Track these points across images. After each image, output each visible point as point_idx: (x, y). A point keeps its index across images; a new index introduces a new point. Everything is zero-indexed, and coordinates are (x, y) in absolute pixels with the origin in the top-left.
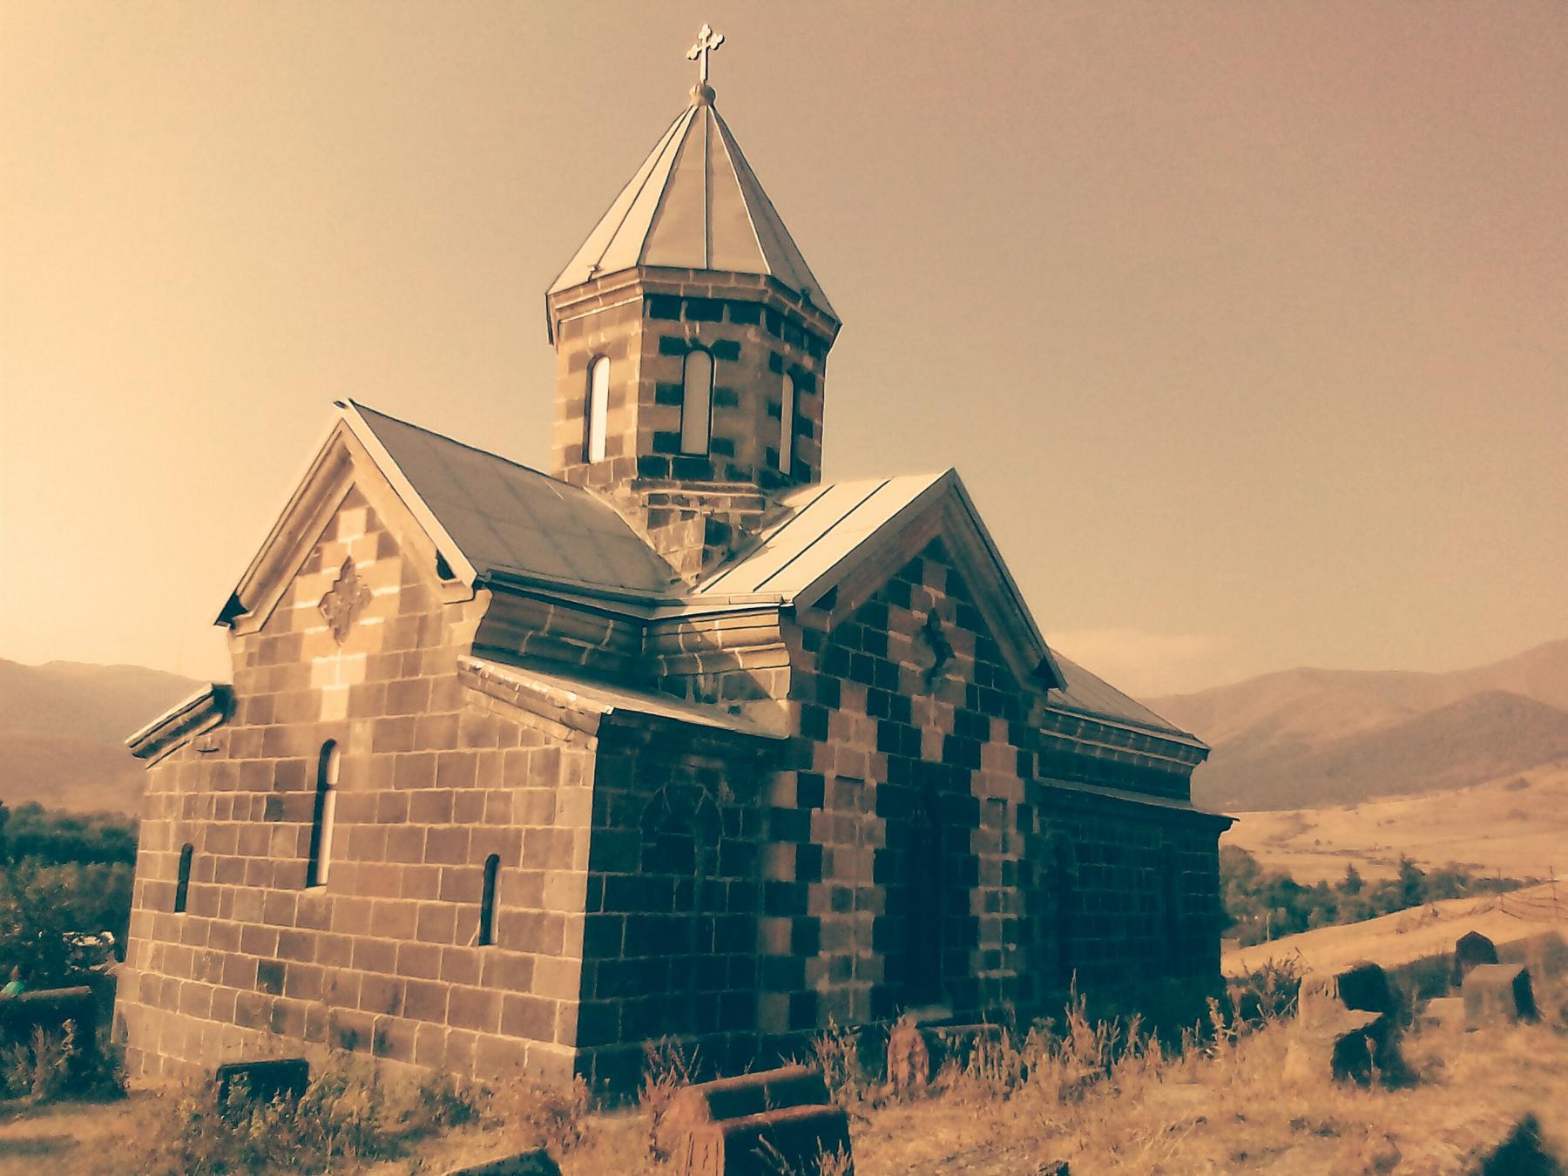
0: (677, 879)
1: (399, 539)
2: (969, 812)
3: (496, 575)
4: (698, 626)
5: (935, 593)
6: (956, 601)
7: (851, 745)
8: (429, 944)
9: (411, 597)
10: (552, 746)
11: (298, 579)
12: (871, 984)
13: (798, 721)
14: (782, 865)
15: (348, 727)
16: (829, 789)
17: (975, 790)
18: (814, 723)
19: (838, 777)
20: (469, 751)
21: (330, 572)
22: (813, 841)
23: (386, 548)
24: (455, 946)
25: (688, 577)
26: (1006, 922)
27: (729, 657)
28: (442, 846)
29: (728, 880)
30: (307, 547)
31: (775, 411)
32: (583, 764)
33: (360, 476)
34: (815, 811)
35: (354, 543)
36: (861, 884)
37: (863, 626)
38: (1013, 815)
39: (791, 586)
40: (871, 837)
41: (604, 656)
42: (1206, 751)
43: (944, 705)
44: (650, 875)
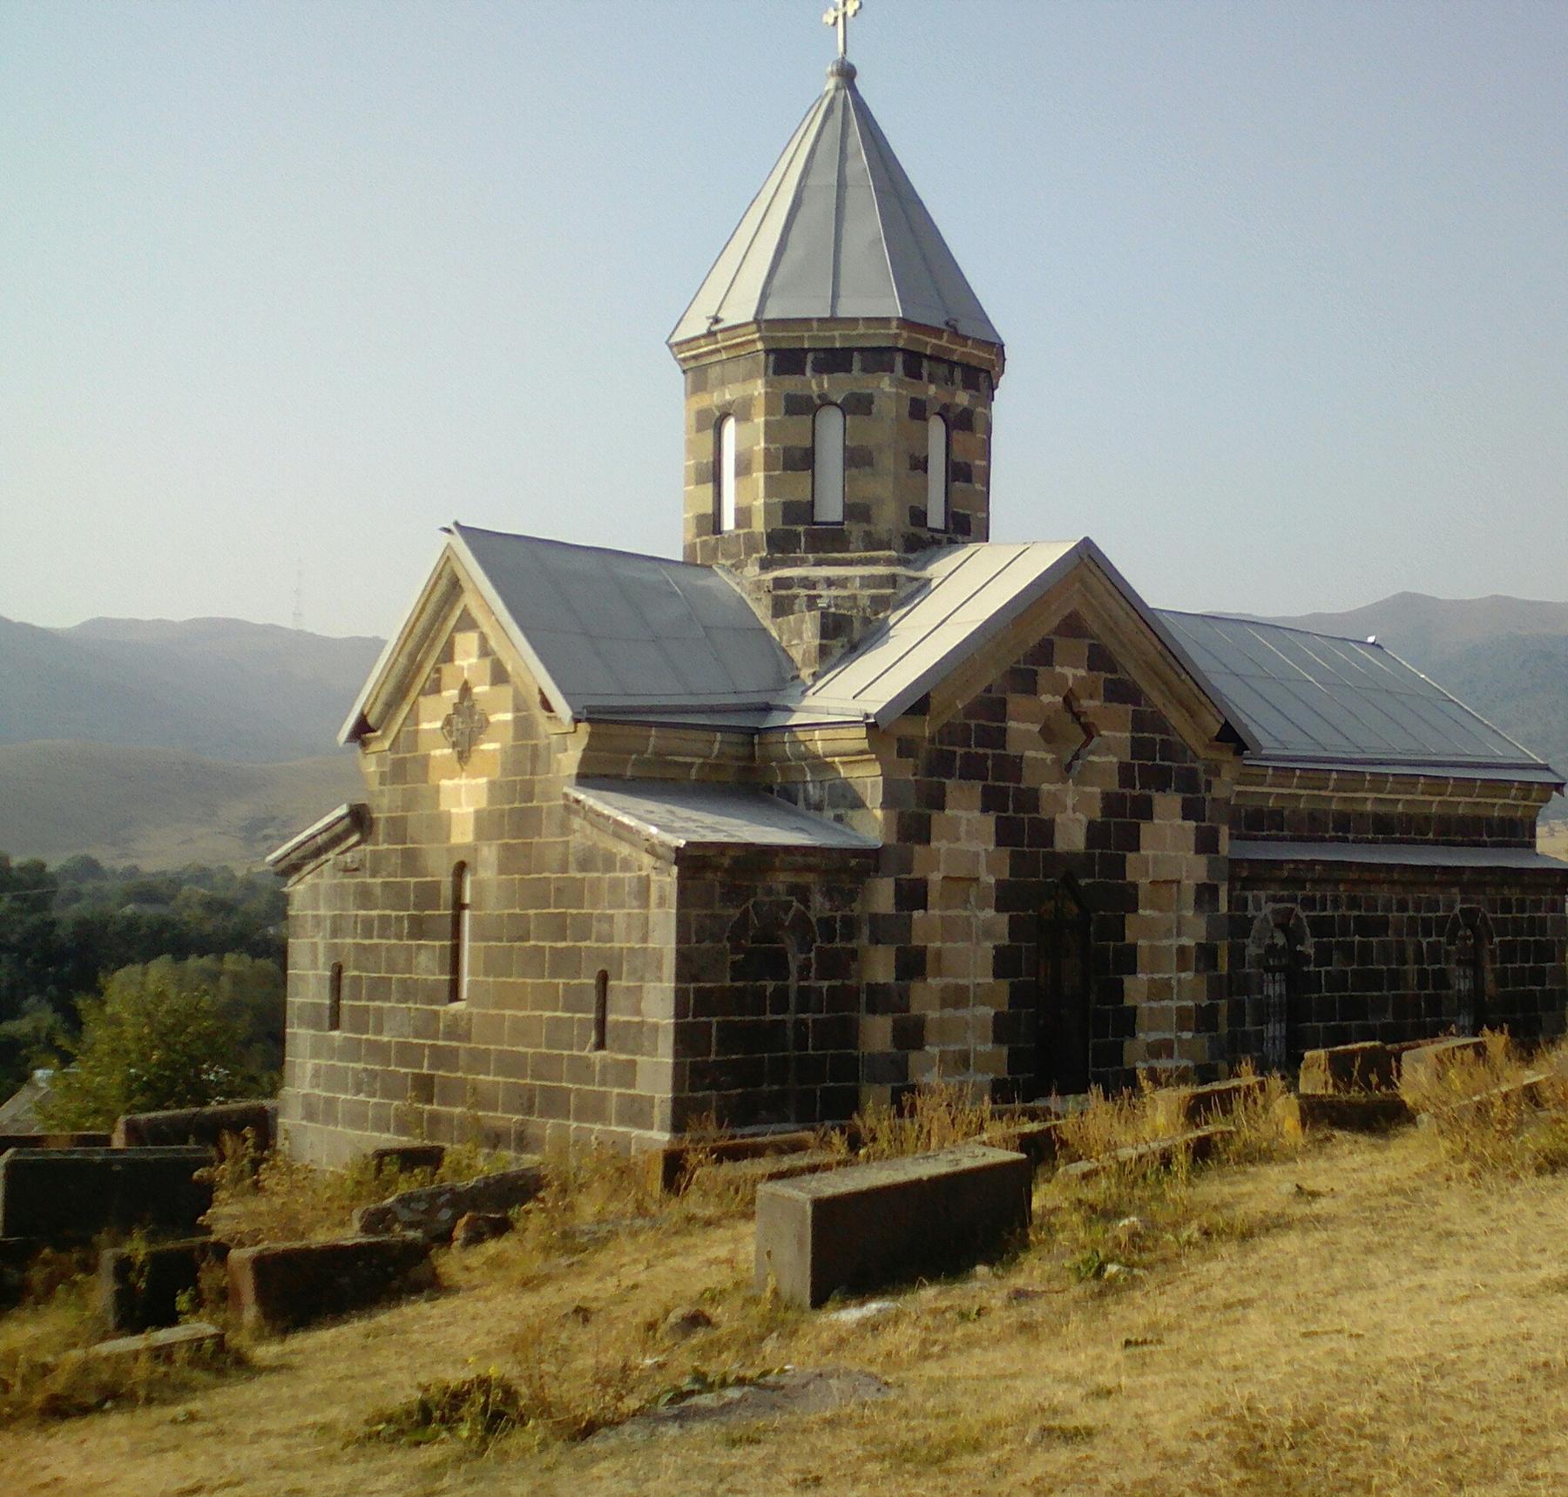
0: (770, 985)
1: (509, 668)
2: (1128, 899)
3: (591, 710)
4: (801, 736)
5: (1072, 673)
6: (1104, 675)
7: (963, 845)
8: (556, 1052)
9: (524, 726)
10: (644, 873)
11: (421, 699)
12: (992, 1076)
13: (895, 828)
14: (880, 967)
15: (476, 850)
16: (933, 895)
18: (914, 828)
20: (579, 875)
21: (451, 694)
22: (915, 943)
23: (499, 676)
24: (575, 1053)
25: (805, 673)
27: (831, 766)
28: (564, 962)
29: (826, 984)
30: (427, 668)
32: (668, 889)
33: (468, 600)
34: (918, 914)
35: (470, 666)
36: (980, 980)
37: (973, 723)
38: (1190, 897)
39: (876, 701)
40: (988, 934)
41: (717, 767)
42: (1559, 787)
43: (1088, 789)
44: (739, 984)
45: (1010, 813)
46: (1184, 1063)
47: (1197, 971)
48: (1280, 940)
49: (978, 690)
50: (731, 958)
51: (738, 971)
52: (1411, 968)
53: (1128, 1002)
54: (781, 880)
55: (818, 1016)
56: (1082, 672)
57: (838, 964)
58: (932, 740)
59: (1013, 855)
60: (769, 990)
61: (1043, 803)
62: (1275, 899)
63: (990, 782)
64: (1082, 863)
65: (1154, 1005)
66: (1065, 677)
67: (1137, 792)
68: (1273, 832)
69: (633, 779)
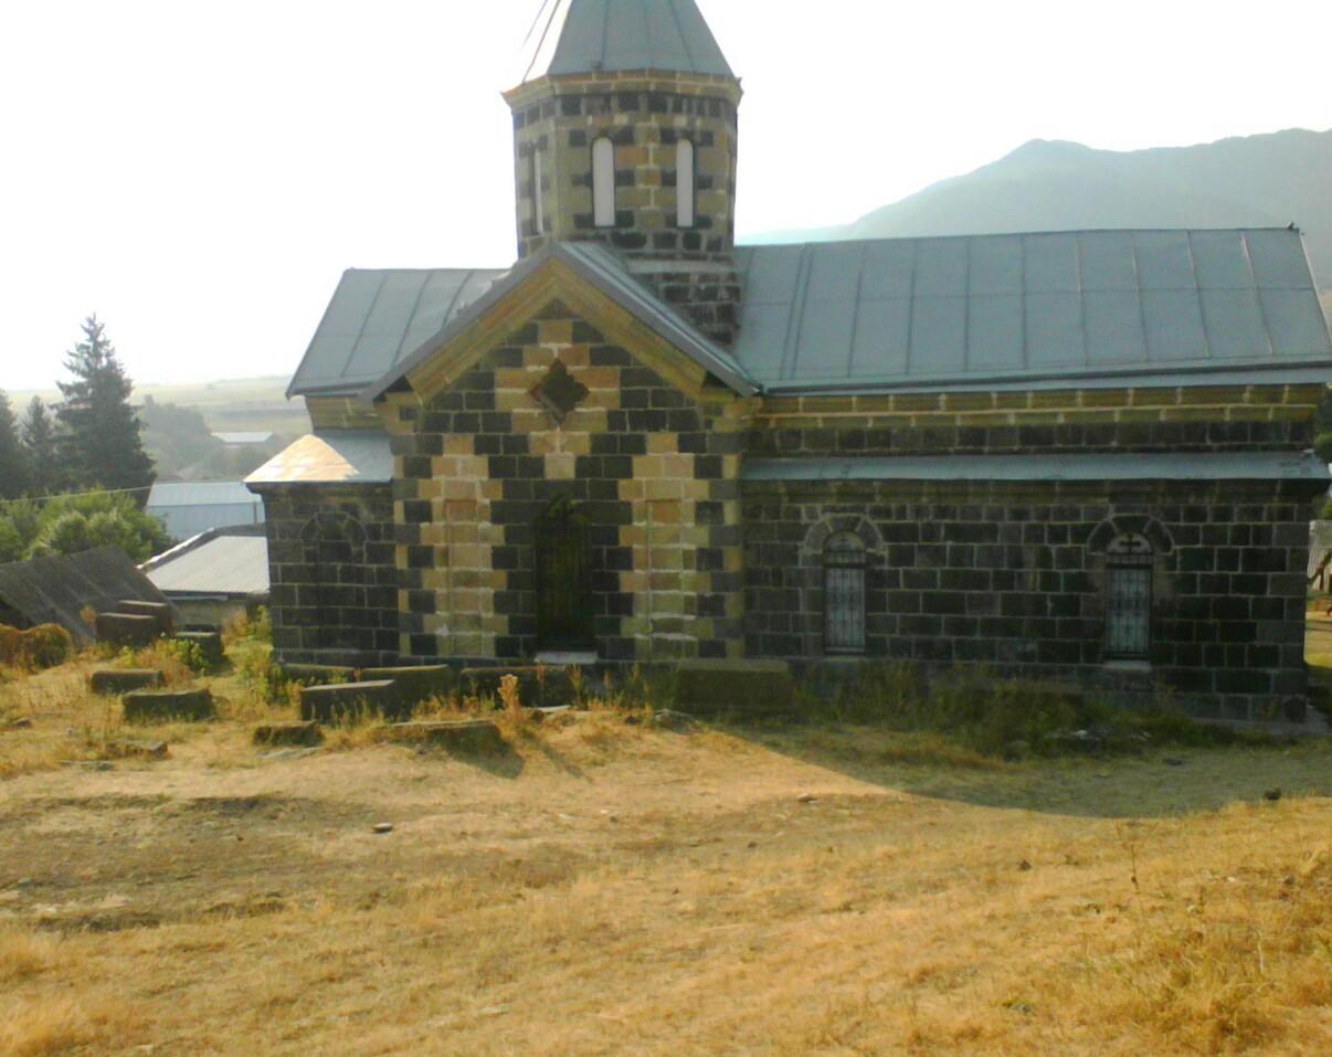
2: (624, 514)
6: (589, 345)
7: (459, 478)
12: (494, 634)
16: (436, 511)
17: (623, 497)
19: (447, 501)
22: (424, 543)
26: (688, 600)
31: (588, 180)
34: (424, 525)
38: (691, 512)
40: (485, 538)
44: (312, 564)
45: (501, 454)
46: (688, 638)
47: (699, 569)
48: (854, 542)
49: (464, 367)
50: (303, 548)
51: (310, 556)
52: (1032, 573)
53: (624, 589)
54: (335, 501)
55: (371, 586)
56: (567, 345)
57: (384, 554)
58: (428, 408)
59: (506, 485)
60: (339, 568)
61: (531, 445)
62: (833, 510)
63: (481, 433)
64: (575, 487)
65: (660, 592)
66: (550, 351)
67: (628, 431)
68: (876, 449)
69: (349, 429)
